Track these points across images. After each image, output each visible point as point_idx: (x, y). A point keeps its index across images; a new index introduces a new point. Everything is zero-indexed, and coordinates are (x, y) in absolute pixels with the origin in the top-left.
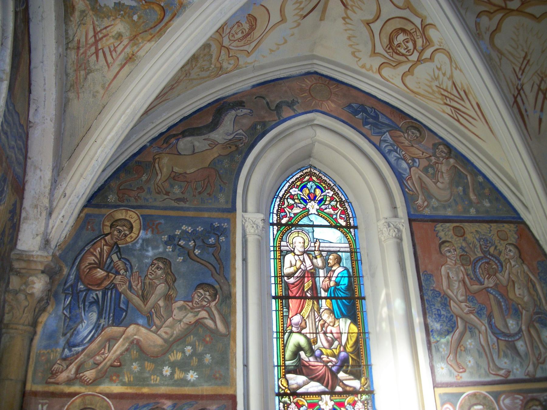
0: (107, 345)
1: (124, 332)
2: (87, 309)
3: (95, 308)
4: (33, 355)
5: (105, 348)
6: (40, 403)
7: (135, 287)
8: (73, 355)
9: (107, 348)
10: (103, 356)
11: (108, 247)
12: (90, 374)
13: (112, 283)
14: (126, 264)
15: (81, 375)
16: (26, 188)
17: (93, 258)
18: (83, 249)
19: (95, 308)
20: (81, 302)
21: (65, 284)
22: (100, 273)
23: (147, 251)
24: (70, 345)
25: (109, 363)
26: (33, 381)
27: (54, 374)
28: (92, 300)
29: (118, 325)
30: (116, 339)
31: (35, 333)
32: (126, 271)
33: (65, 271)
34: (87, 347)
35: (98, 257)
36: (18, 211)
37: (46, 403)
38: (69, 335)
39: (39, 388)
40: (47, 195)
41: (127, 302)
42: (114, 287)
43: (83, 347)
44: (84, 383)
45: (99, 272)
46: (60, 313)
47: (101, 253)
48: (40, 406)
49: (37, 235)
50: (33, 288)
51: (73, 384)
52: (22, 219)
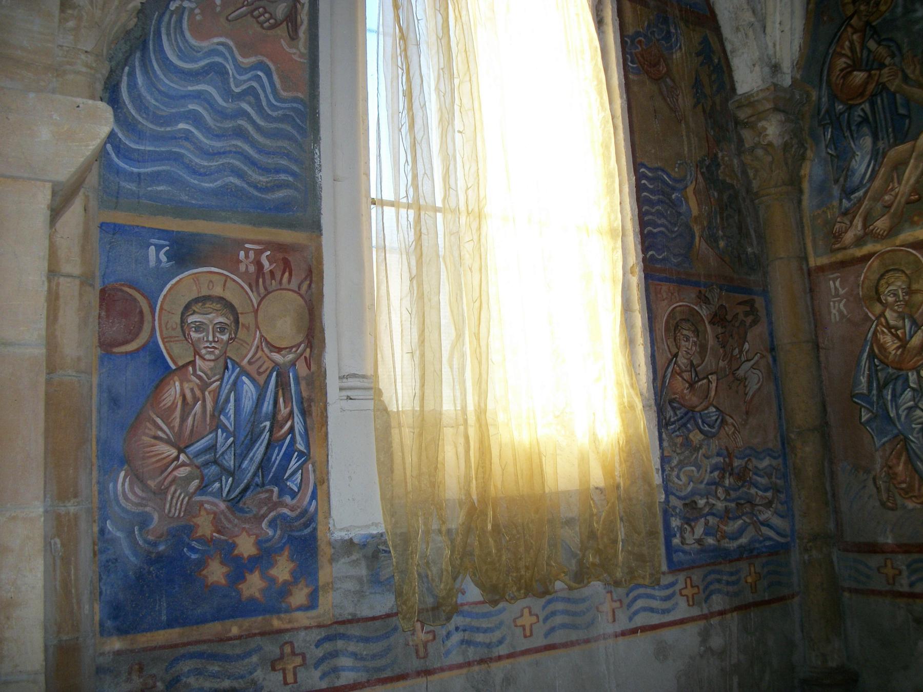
0: (895, 176)
1: (914, 147)
2: (855, 135)
3: (865, 129)
4: (807, 221)
5: (892, 181)
6: (830, 279)
7: (911, 76)
8: (855, 204)
9: (896, 180)
10: (893, 193)
11: (859, 34)
12: (881, 224)
13: (878, 84)
14: (889, 47)
15: (871, 228)
16: (717, 12)
17: (844, 59)
18: (827, 53)
19: (865, 129)
20: (845, 129)
21: (819, 114)
22: (859, 76)
23: (915, 11)
24: (847, 193)
25: (903, 200)
26: (815, 253)
27: (838, 237)
28: (859, 119)
29: (903, 143)
30: (905, 163)
31: (801, 191)
32: (893, 56)
33: (814, 95)
34: (869, 188)
35: (849, 54)
36: (716, 46)
37: (837, 278)
38: (842, 179)
39: (824, 260)
40: (746, 6)
41: (907, 103)
42: (883, 88)
43: (864, 190)
44: (878, 237)
45: (856, 76)
46: (824, 154)
47: (852, 49)
48: (831, 282)
49: (754, 65)
50: (767, 135)
51: (865, 244)
52: (729, 54)
